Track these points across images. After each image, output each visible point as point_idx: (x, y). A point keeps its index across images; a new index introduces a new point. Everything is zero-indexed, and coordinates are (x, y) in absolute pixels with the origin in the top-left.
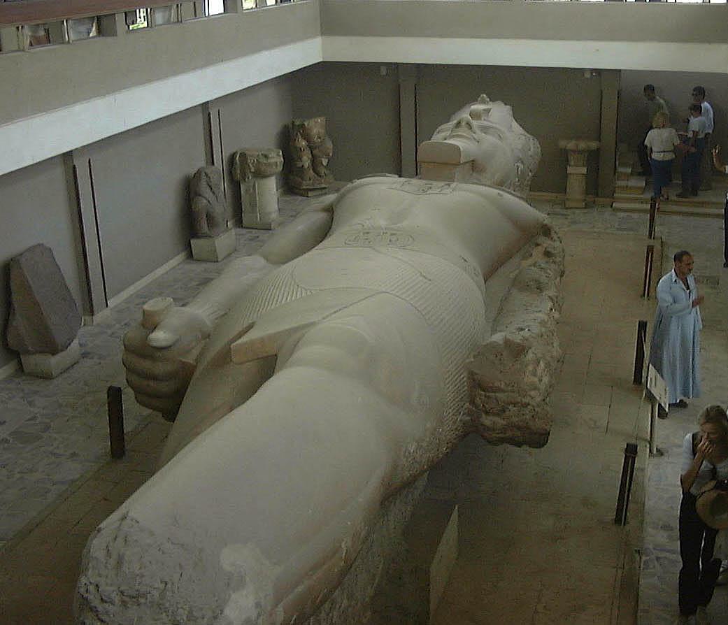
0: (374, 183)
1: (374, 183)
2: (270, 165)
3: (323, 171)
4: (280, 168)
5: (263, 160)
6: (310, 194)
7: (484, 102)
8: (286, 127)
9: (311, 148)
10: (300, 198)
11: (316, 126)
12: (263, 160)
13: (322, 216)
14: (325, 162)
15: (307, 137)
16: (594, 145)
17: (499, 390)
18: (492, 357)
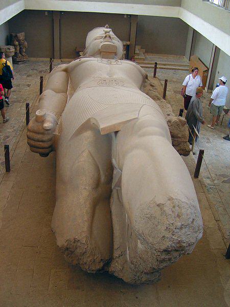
0: (92, 60)
1: (92, 60)
2: (11, 52)
3: (24, 54)
4: (13, 54)
5: (8, 51)
6: (20, 63)
7: (107, 28)
8: (7, 36)
9: (20, 45)
10: (16, 65)
11: (21, 36)
12: (8, 51)
13: (64, 73)
14: (24, 50)
15: (19, 41)
16: (128, 43)
17: (179, 137)
18: (176, 126)
